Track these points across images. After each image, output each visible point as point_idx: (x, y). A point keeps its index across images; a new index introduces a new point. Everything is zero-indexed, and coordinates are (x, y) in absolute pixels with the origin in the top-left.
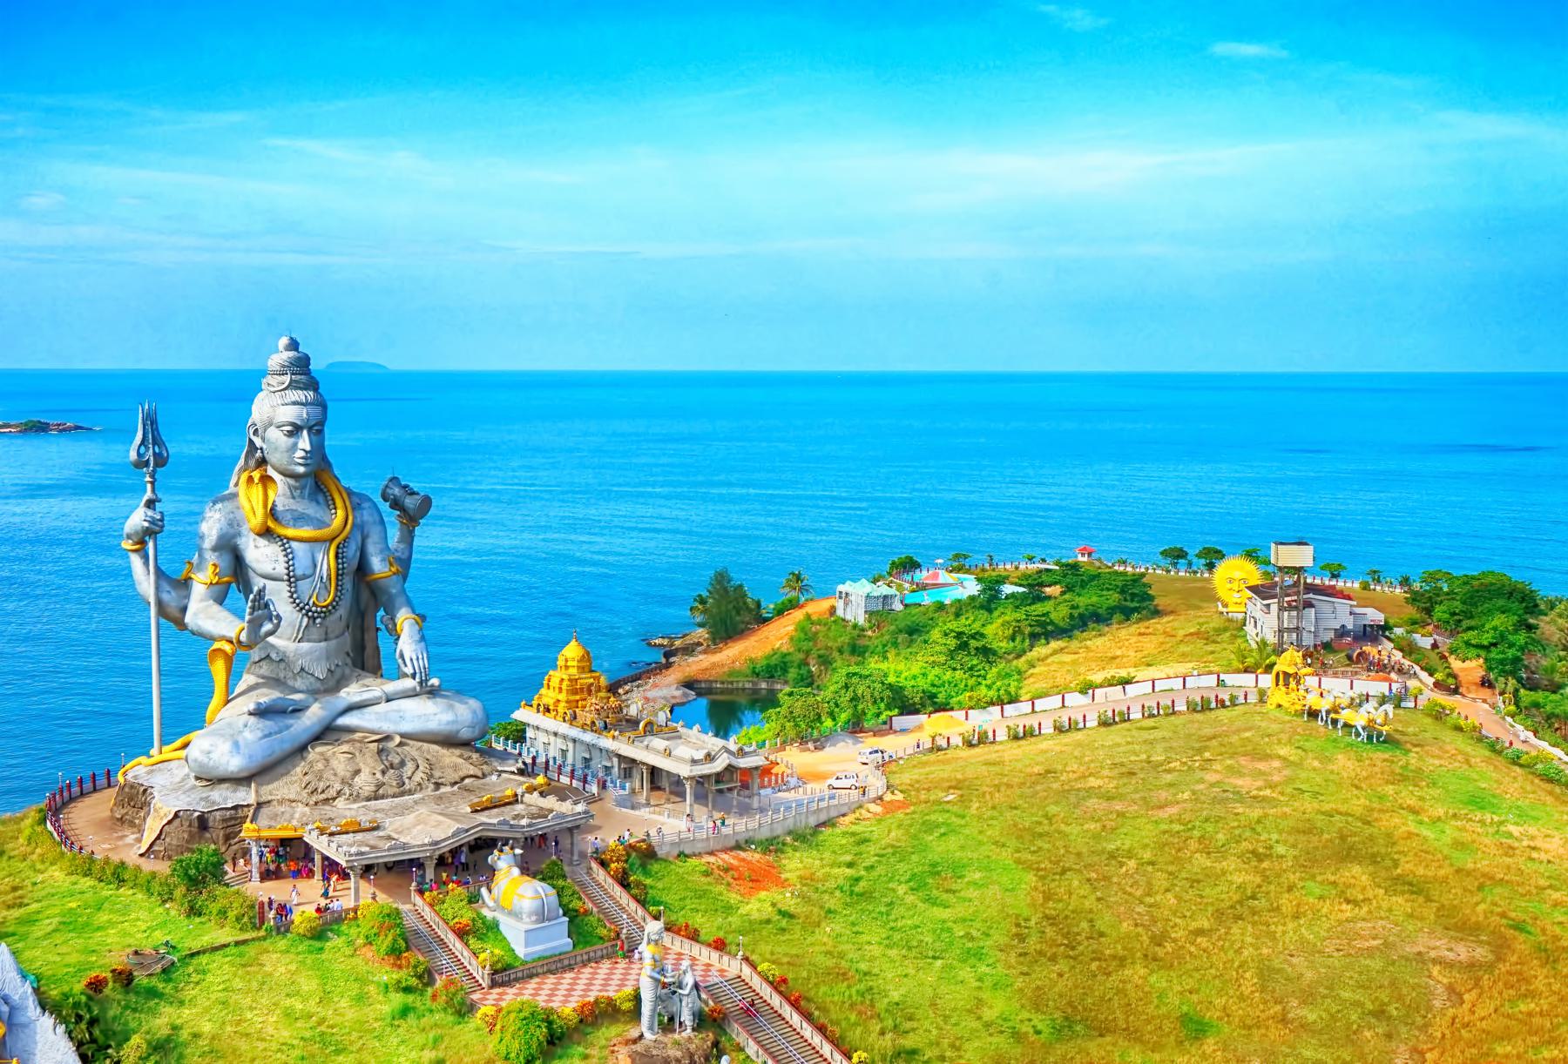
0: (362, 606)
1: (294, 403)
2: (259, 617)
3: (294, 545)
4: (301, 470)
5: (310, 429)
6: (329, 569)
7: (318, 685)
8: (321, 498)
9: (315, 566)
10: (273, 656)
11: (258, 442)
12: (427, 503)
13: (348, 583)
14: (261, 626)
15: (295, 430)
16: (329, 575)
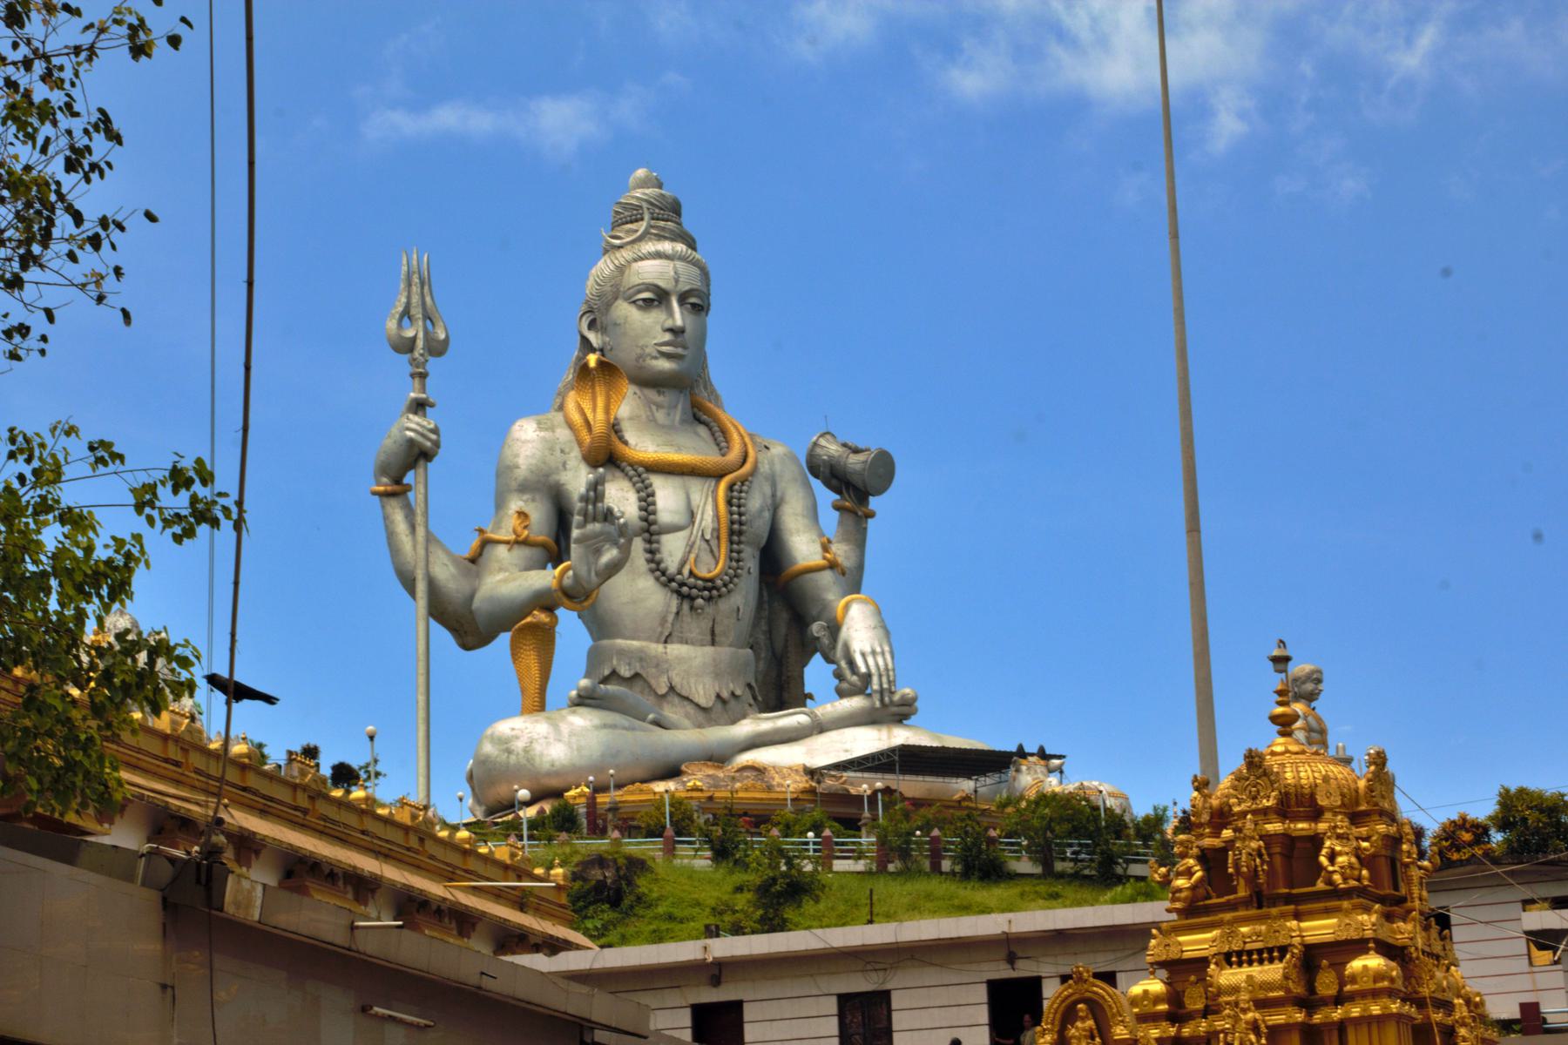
0: (779, 644)
1: (659, 255)
2: (596, 536)
4: (665, 365)
5: (682, 299)
6: (717, 516)
7: (701, 717)
8: (702, 430)
9: (692, 515)
10: (625, 672)
11: (593, 337)
12: (883, 470)
13: (751, 562)
14: (598, 552)
15: (658, 298)
16: (717, 530)
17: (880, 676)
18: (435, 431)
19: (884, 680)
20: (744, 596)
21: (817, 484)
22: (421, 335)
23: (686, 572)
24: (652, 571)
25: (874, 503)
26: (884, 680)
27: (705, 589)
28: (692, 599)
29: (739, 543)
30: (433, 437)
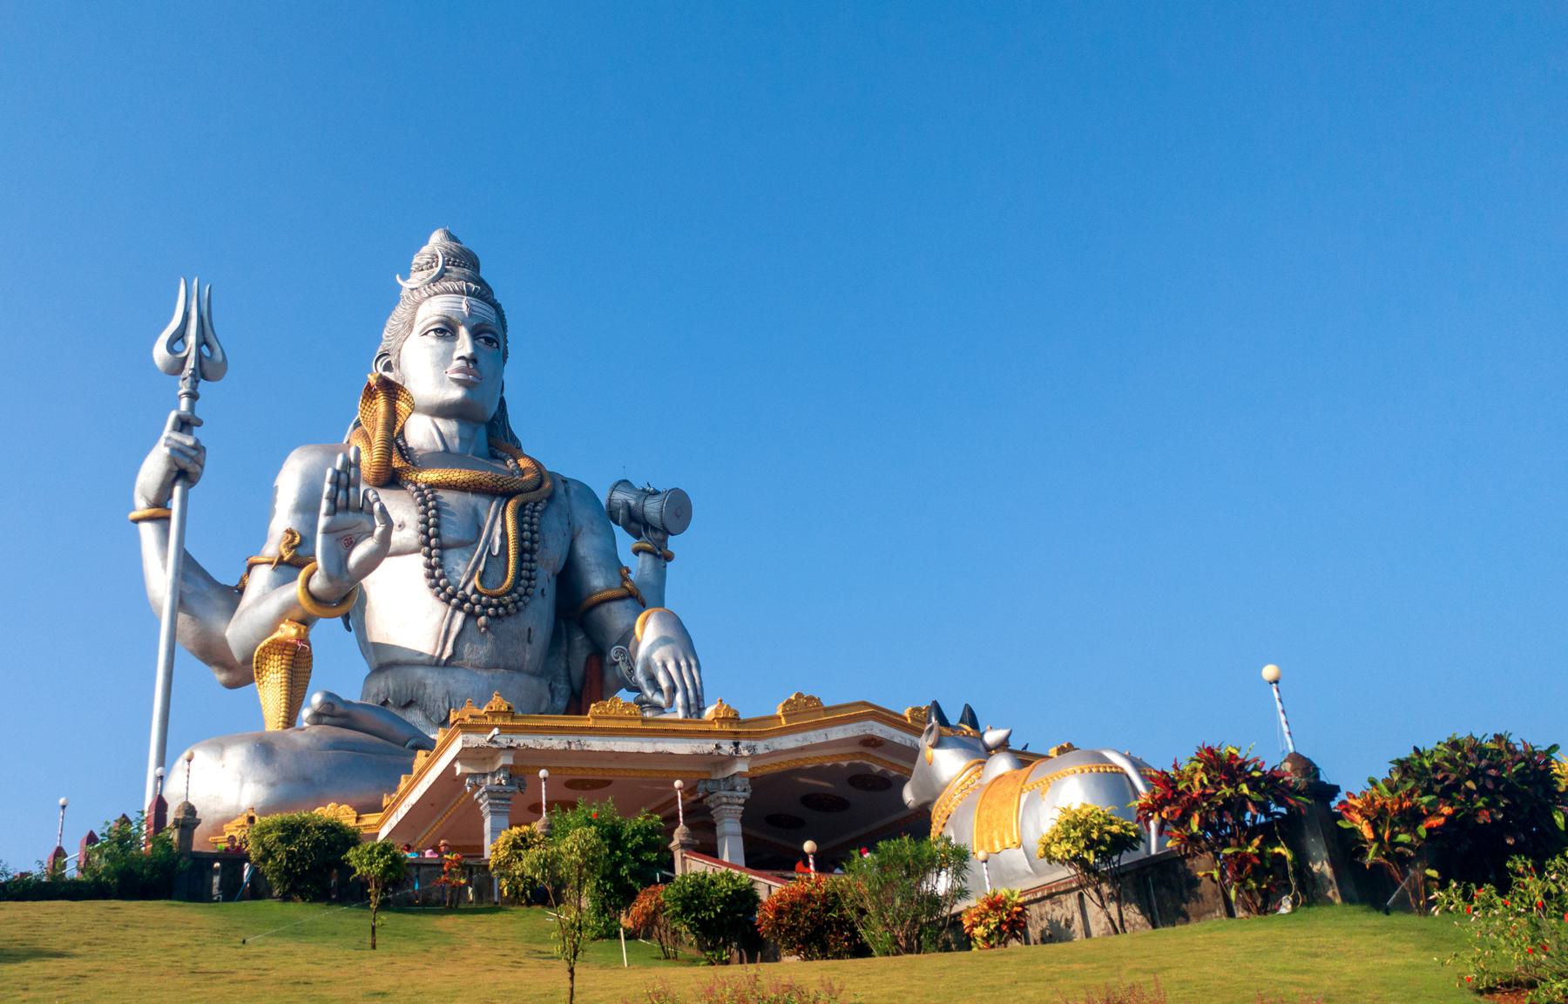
3: (440, 493)
6: (504, 535)
9: (479, 530)
12: (680, 508)
17: (686, 690)
18: (197, 447)
19: (691, 693)
20: (539, 615)
21: (619, 531)
22: (193, 354)
23: (469, 590)
24: (432, 587)
25: (673, 543)
26: (691, 693)
27: (491, 605)
28: (478, 616)
29: (531, 561)
30: (193, 453)
